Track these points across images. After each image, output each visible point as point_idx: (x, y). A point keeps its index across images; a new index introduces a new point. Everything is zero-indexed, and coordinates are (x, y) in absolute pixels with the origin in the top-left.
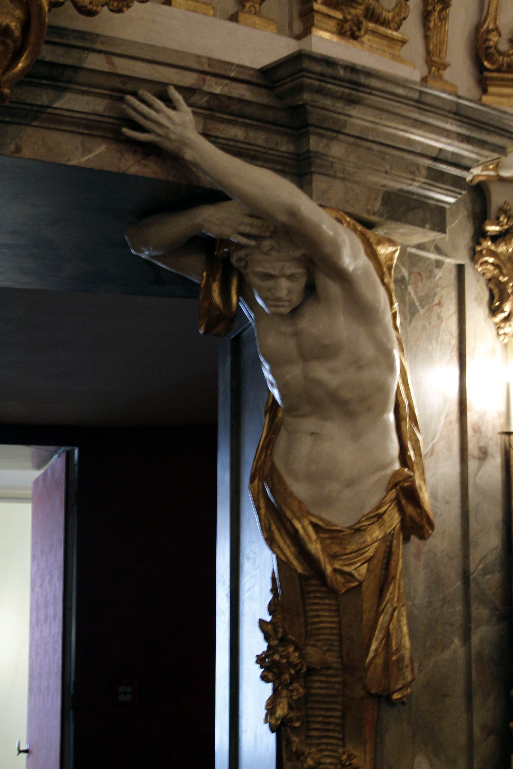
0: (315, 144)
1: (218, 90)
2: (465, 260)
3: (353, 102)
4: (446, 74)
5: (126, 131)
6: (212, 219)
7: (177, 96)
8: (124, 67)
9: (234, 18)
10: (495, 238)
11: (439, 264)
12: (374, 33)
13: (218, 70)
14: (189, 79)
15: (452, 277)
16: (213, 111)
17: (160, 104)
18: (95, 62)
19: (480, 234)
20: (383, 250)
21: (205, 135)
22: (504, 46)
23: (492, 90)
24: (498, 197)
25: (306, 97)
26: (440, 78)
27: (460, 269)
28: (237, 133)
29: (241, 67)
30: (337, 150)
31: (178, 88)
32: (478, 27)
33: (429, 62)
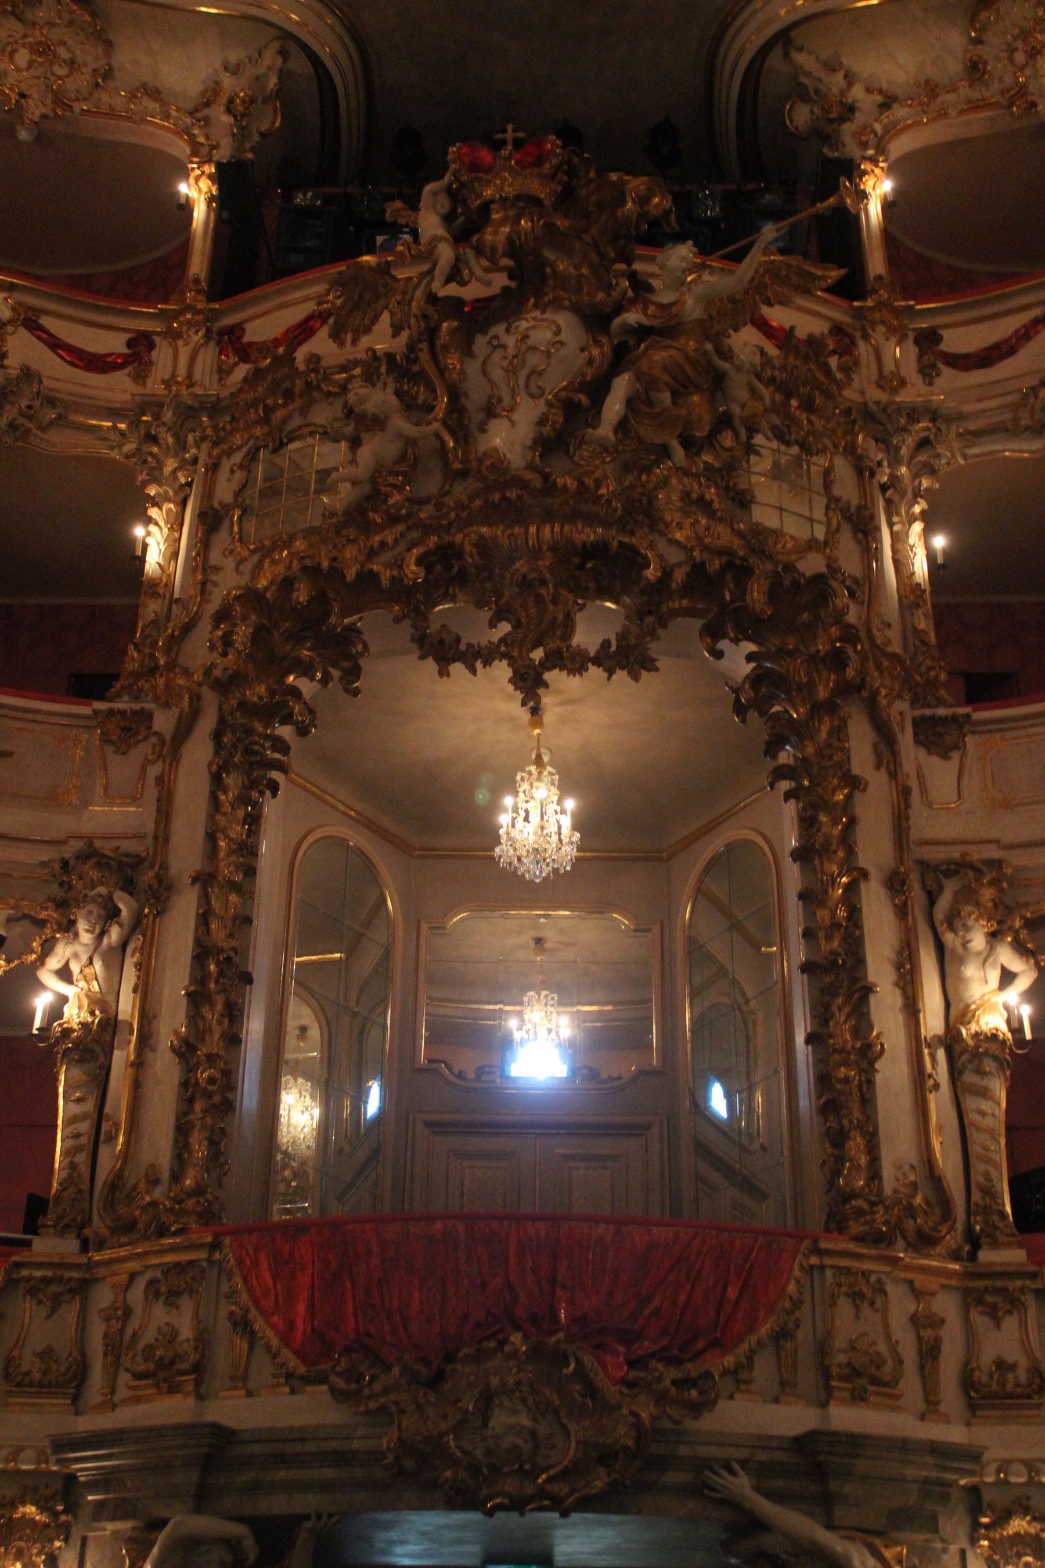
0: (833, 1486)
1: (764, 1458)
2: (964, 1544)
3: (857, 1456)
4: (942, 1408)
5: (706, 1492)
6: (768, 1542)
7: (736, 1467)
8: (703, 1451)
9: (776, 1401)
10: (987, 1527)
11: (945, 1550)
12: (877, 1394)
13: (765, 1442)
14: (745, 1453)
15: (957, 1559)
16: (763, 1472)
17: (725, 1474)
18: (684, 1450)
19: (976, 1525)
20: (888, 1554)
21: (758, 1489)
22: (985, 1379)
23: (978, 1413)
24: (987, 1496)
25: (821, 1458)
26: (936, 1411)
27: (963, 1553)
28: (780, 1483)
29: (780, 1438)
30: (848, 1488)
31: (738, 1461)
32: (967, 1364)
33: (927, 1401)
